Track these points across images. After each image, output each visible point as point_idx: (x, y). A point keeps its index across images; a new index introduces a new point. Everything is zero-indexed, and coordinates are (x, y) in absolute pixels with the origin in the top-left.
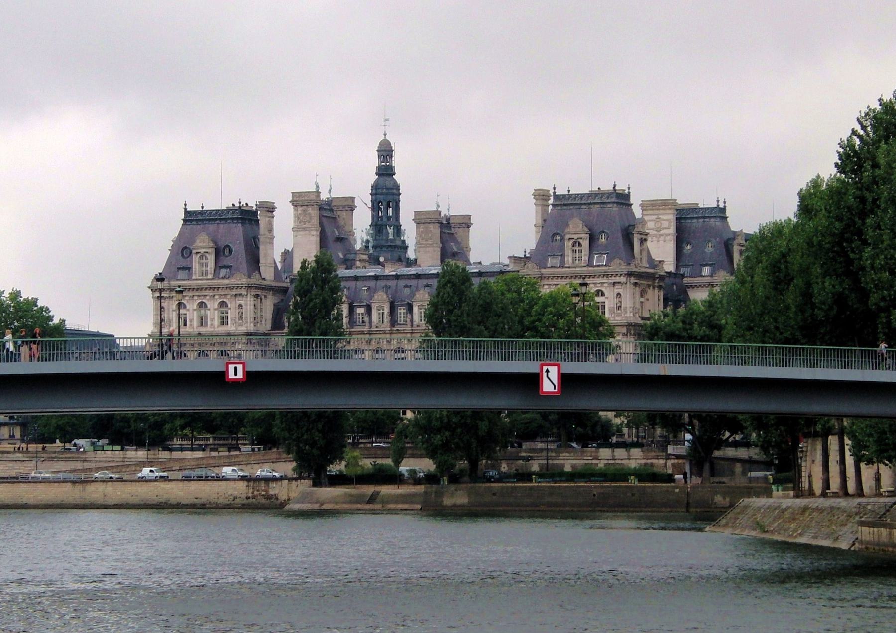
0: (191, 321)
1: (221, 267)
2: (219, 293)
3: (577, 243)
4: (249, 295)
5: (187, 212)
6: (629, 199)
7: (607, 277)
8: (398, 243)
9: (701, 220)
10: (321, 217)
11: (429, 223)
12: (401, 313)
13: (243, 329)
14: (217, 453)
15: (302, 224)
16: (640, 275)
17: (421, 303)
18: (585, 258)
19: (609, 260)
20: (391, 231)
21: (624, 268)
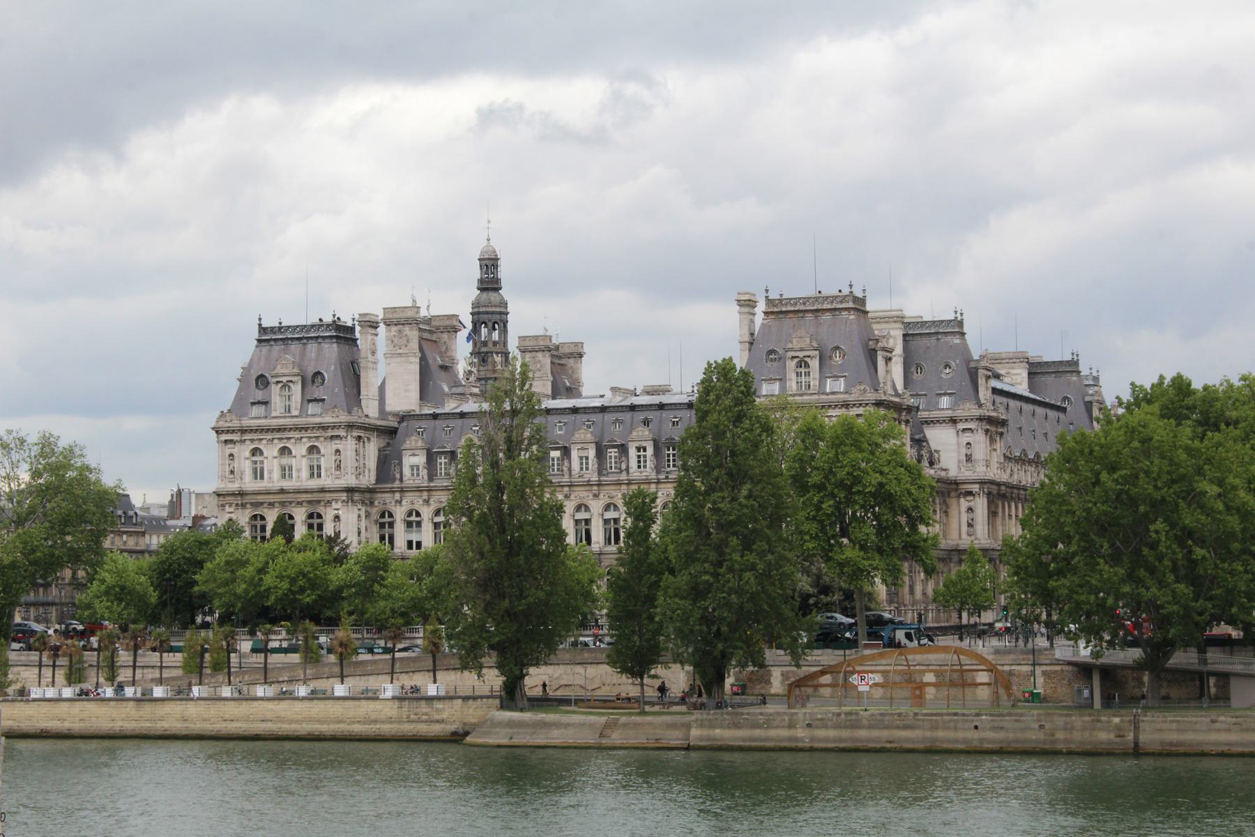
0: (270, 472)
1: (310, 401)
2: (308, 435)
3: (803, 363)
4: (349, 436)
5: (263, 330)
6: (864, 304)
7: (847, 408)
10: (421, 338)
11: (537, 351)
13: (342, 483)
15: (397, 348)
17: (582, 445)
18: (814, 383)
19: (848, 385)
20: (498, 359)
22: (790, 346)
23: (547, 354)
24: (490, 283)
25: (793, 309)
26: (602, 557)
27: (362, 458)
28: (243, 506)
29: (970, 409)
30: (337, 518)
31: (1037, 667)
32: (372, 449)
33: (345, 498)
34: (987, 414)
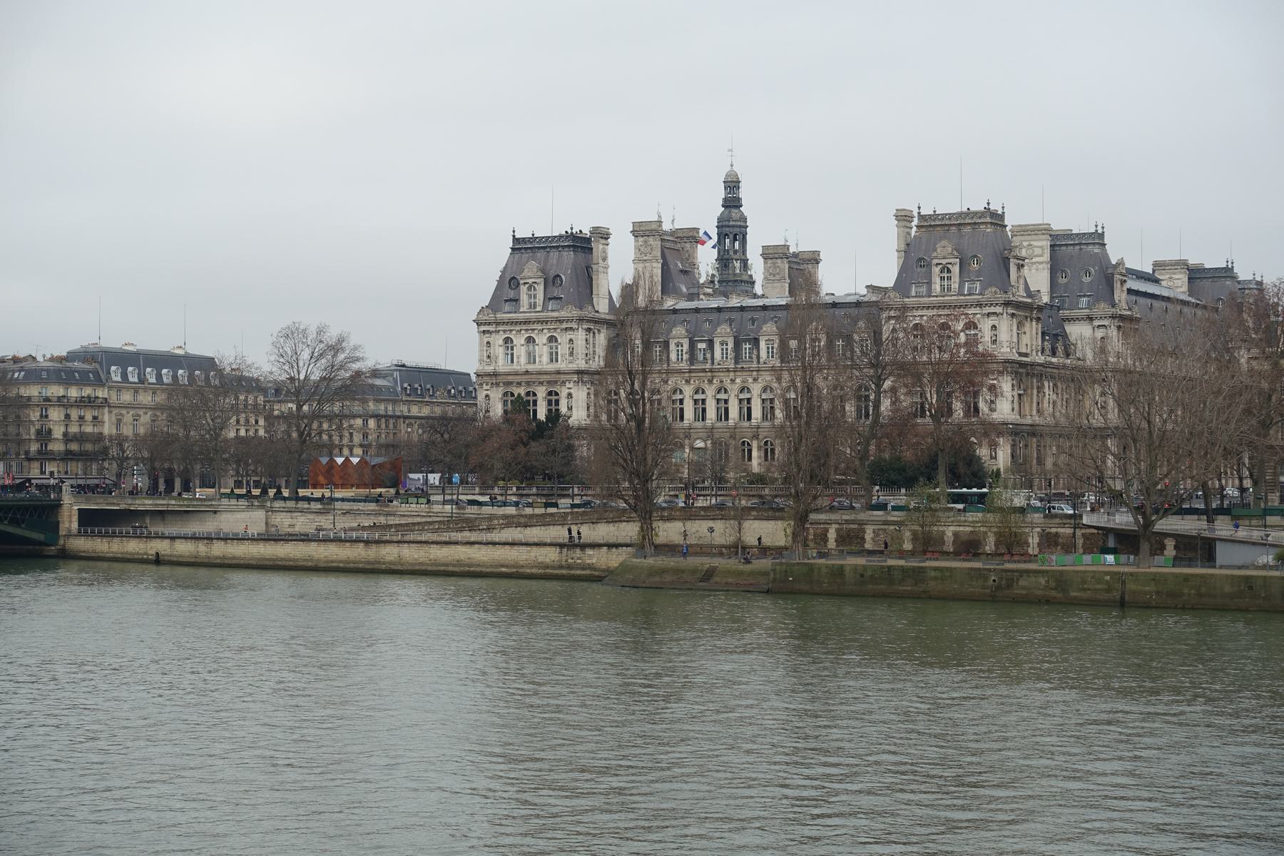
1: (550, 299)
5: (516, 240)
6: (1003, 220)
7: (981, 307)
8: (745, 278)
9: (1078, 247)
10: (663, 248)
12: (746, 349)
13: (573, 367)
14: (531, 509)
16: (1018, 306)
18: (955, 286)
19: (983, 289)
20: (737, 264)
21: (1002, 297)
22: (935, 254)
23: (786, 260)
24: (732, 202)
25: (940, 223)
26: (759, 430)
27: (591, 346)
28: (497, 384)
29: (1103, 308)
30: (570, 395)
31: (1077, 530)
32: (602, 339)
33: (576, 379)
34: (1119, 313)
